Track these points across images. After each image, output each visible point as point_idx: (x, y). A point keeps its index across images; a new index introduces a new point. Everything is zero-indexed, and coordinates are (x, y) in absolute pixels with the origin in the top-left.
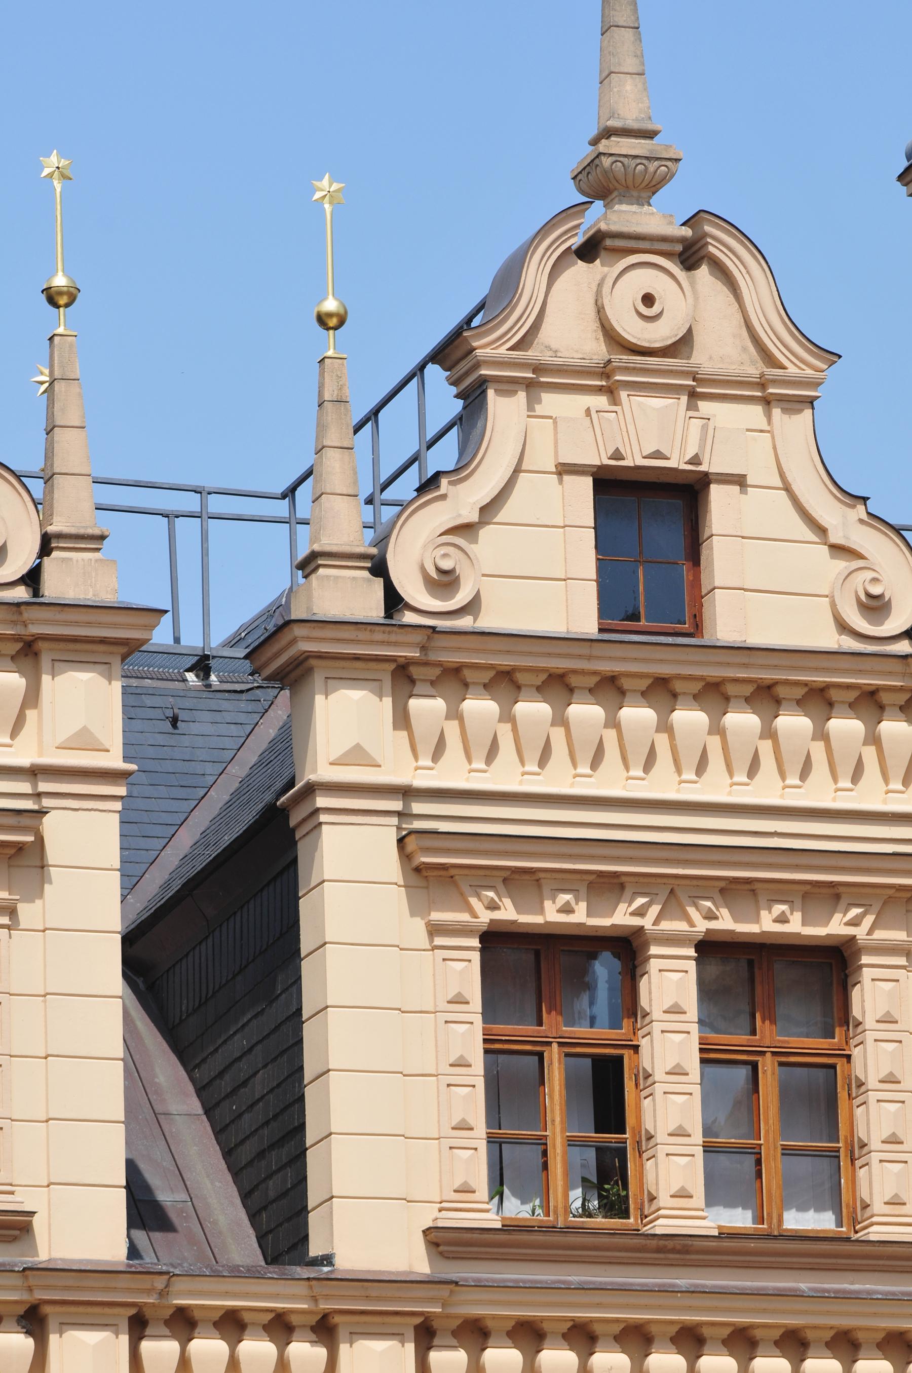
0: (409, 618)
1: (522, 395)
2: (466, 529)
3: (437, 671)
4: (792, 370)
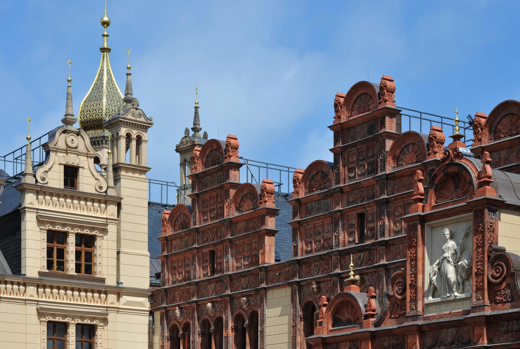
0: (39, 184)
1: (55, 153)
2: (46, 172)
3: (42, 192)
4: (91, 152)
